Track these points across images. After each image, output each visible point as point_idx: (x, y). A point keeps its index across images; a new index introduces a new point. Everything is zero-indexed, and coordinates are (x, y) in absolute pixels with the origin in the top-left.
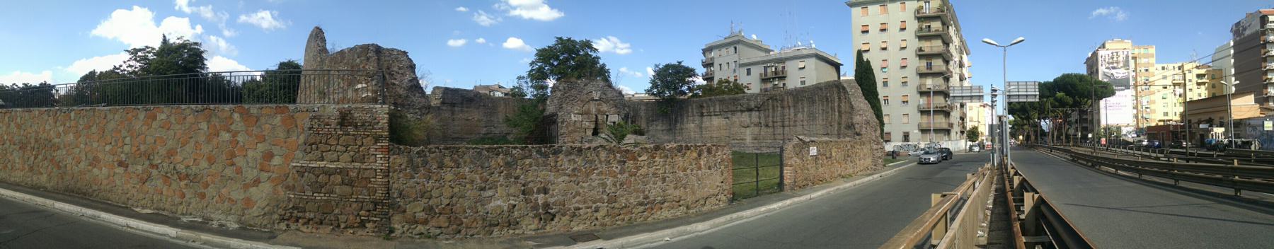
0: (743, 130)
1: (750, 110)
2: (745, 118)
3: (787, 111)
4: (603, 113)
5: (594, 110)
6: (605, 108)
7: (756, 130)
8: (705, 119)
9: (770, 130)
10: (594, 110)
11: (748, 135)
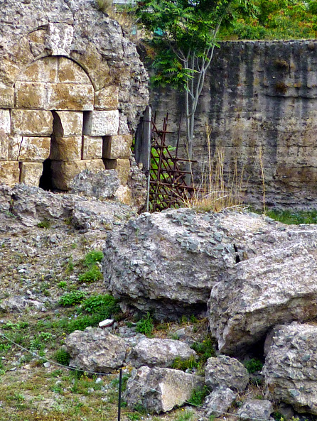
4: (75, 104)
5: (46, 97)
6: (80, 86)
8: (287, 107)
10: (46, 97)
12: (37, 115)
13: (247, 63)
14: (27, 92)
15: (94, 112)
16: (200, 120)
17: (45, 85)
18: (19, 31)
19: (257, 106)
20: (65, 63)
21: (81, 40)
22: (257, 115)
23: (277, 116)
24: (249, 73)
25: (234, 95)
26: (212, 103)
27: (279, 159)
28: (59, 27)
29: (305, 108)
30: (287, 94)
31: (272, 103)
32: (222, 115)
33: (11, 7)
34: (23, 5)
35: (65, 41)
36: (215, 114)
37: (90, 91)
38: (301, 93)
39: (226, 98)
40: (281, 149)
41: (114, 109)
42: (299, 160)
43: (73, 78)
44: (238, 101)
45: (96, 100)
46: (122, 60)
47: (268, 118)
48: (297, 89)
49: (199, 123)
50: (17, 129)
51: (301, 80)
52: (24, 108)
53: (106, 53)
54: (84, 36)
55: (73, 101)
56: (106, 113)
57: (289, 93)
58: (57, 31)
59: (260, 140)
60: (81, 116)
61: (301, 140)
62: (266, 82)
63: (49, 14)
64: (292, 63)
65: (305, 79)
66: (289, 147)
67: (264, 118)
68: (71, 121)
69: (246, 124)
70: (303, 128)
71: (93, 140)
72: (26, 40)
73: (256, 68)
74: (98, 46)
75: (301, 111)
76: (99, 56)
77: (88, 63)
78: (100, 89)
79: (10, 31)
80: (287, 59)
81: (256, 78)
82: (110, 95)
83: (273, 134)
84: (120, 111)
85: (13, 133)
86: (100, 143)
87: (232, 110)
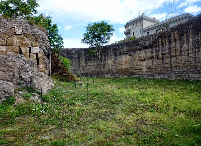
0: (141, 62)
1: (145, 48)
2: (142, 54)
3: (173, 44)
4: (26, 45)
7: (150, 62)
8: (118, 57)
9: (160, 61)
12: (14, 47)
13: (110, 49)
14: (10, 42)
15: (32, 47)
17: (16, 41)
18: (6, 28)
19: (112, 58)
20: (22, 36)
21: (25, 31)
22: (113, 59)
24: (110, 51)
25: (108, 56)
26: (104, 58)
27: (117, 68)
28: (18, 27)
29: (121, 57)
30: (117, 54)
31: (115, 56)
32: (106, 60)
33: (2, 22)
34: (7, 23)
35: (20, 30)
36: (105, 60)
37: (30, 42)
38: (120, 54)
39: (107, 57)
40: (117, 66)
41: (37, 47)
43: (24, 39)
44: (109, 57)
45: (32, 45)
46: (37, 35)
47: (114, 60)
48: (119, 53)
50: (7, 50)
52: (10, 46)
53: (33, 34)
54: (26, 30)
55: (25, 44)
56: (35, 48)
57: (118, 54)
58: (17, 28)
59: (113, 64)
60: (28, 49)
62: (113, 53)
63: (15, 25)
64: (118, 48)
65: (120, 50)
68: (25, 49)
69: (111, 61)
71: (32, 54)
72: (9, 30)
73: (111, 50)
74: (30, 32)
76: (31, 34)
77: (28, 36)
78: (33, 42)
79: (3, 28)
80: (116, 47)
81: (112, 52)
82: (36, 43)
83: (115, 63)
84: (40, 47)
85: (6, 51)
86: (35, 55)
87: (108, 59)
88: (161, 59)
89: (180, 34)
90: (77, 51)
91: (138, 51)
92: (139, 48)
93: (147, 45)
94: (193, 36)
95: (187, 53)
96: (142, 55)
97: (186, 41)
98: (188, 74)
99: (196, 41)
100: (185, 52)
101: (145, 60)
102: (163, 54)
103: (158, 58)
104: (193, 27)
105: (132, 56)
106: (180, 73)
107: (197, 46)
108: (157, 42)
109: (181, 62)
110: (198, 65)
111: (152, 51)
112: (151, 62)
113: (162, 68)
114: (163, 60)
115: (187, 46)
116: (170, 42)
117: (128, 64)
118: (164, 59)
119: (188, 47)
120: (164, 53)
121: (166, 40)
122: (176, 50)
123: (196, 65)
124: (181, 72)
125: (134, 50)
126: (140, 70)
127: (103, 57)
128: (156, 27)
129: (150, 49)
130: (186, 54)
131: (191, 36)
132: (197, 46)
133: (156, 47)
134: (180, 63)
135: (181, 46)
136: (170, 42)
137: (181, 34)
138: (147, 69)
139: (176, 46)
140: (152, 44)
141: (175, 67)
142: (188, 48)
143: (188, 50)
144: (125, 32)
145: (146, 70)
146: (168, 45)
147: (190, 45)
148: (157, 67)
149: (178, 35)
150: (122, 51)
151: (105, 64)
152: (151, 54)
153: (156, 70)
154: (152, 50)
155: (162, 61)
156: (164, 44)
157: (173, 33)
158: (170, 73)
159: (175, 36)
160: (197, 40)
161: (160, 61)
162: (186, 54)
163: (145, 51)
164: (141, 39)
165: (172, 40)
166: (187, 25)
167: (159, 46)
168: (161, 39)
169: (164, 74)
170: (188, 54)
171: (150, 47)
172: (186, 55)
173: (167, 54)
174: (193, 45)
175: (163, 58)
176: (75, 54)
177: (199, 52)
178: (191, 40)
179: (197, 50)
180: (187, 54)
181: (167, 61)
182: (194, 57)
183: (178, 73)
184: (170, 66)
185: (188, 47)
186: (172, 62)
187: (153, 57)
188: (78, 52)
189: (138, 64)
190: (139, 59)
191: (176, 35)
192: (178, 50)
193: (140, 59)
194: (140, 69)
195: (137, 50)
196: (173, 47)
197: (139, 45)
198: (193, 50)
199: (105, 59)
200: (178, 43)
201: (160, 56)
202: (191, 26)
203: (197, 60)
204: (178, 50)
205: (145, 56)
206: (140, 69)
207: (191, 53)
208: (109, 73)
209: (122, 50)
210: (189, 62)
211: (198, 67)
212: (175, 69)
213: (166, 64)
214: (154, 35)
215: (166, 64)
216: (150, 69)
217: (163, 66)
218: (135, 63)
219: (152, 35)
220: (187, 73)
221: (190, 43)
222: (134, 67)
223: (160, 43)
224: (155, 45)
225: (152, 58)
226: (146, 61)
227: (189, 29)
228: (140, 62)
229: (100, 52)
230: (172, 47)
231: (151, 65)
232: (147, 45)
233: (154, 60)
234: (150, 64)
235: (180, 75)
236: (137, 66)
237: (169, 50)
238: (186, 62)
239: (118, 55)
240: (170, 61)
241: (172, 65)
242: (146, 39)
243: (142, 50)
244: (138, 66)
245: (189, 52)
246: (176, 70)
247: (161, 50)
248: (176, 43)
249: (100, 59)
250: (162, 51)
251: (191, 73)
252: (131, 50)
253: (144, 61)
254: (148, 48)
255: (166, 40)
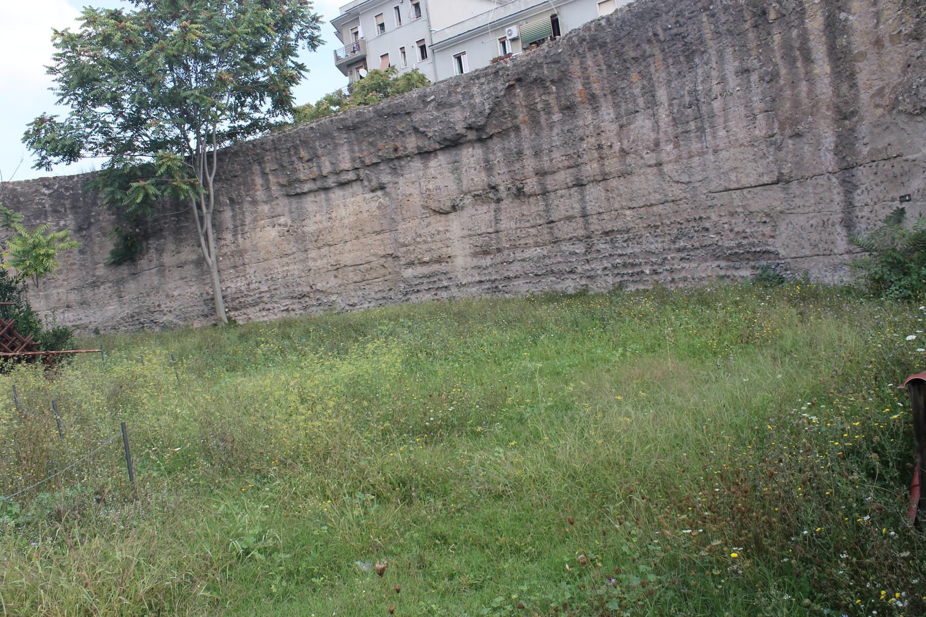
0: (438, 223)
1: (453, 143)
3: (586, 117)
7: (483, 215)
8: (309, 203)
9: (534, 207)
11: (457, 237)
13: (260, 164)
16: (225, 239)
19: (279, 210)
22: (282, 220)
23: (301, 217)
24: (264, 174)
25: (254, 202)
26: (234, 217)
29: (327, 200)
32: (246, 229)
38: (319, 184)
39: (247, 206)
42: (332, 262)
47: (293, 221)
49: (223, 242)
51: (315, 169)
61: (329, 238)
65: (319, 167)
66: (319, 248)
67: (289, 222)
69: (272, 233)
70: (329, 224)
75: (324, 204)
88: (536, 195)
89: (609, 66)
90: (67, 189)
91: (417, 164)
92: (418, 148)
93: (460, 128)
94: (669, 74)
95: (653, 162)
96: (439, 182)
97: (641, 102)
98: (668, 267)
99: (687, 99)
100: (642, 158)
101: (454, 208)
102: (541, 174)
103: (520, 194)
104: (666, 30)
105: (386, 194)
106: (633, 265)
107: (692, 125)
108: (506, 107)
109: (630, 208)
110: (709, 218)
111: (487, 161)
112: (487, 217)
113: (545, 244)
114: (544, 200)
115: (648, 124)
116: (569, 109)
117: (369, 240)
118: (552, 195)
119: (654, 131)
120: (546, 165)
121: (552, 100)
122: (600, 147)
123: (701, 218)
124: (635, 255)
125: (392, 160)
126: (435, 267)
127: (228, 214)
128: (499, 26)
129: (477, 145)
130: (650, 166)
131: (663, 75)
132: (692, 125)
133: (503, 134)
134: (628, 212)
135: (621, 127)
136: (569, 109)
137: (614, 69)
138: (475, 255)
139: (599, 127)
140: (481, 121)
141: (606, 233)
142: (653, 136)
143: (657, 144)
144: (337, 58)
145: (469, 259)
146: (563, 122)
147: (663, 113)
148: (523, 242)
149: (605, 73)
150: (327, 168)
151: (241, 253)
152: (483, 174)
153: (519, 255)
154: (485, 153)
155: (541, 208)
156: (543, 118)
157: (577, 61)
158: (587, 267)
159: (588, 78)
160: (690, 93)
161: (534, 209)
162: (650, 166)
163: (453, 159)
164: (425, 96)
165: (580, 99)
166: (640, 22)
167: (517, 129)
168: (527, 96)
169: (561, 273)
170: (659, 164)
171: (472, 135)
172: (649, 170)
173: (562, 172)
174: (674, 119)
175: (545, 193)
176: (55, 211)
177: (707, 153)
178: (662, 94)
179: (695, 146)
180: (656, 165)
181: (565, 204)
182: (685, 178)
183: (625, 265)
184: (581, 232)
185: (656, 128)
186: (589, 208)
187: (494, 188)
188: (75, 198)
189: (422, 232)
190: (425, 207)
191: (593, 73)
192: (611, 146)
193: (434, 205)
194: (439, 260)
195: (407, 156)
196: (587, 133)
197: (416, 130)
198: (677, 146)
199: (238, 222)
200: (607, 112)
201: (532, 185)
202: (660, 32)
203: (702, 193)
204: (611, 146)
205: (453, 186)
206: (439, 260)
207: (670, 161)
208: (272, 297)
209: (327, 164)
210: (670, 207)
211: (707, 230)
212: (607, 246)
213: (560, 220)
214: (486, 75)
215: (560, 220)
216: (486, 253)
217: (551, 234)
218: (408, 229)
219: (478, 77)
220: (665, 259)
221: (661, 110)
222: (404, 249)
223: (522, 115)
224: (496, 127)
225: (489, 194)
226: (466, 213)
227: (649, 41)
228: (434, 219)
229: (206, 185)
230: (580, 132)
231: (491, 230)
232: (460, 128)
233: (505, 204)
234: (484, 229)
235: (632, 275)
236: (419, 243)
237: (571, 152)
238: (652, 205)
239: (310, 191)
240: (577, 206)
241: (592, 228)
242: (450, 94)
243: (436, 156)
244: (425, 242)
245: (664, 157)
246: (611, 251)
247: (528, 152)
248: (596, 110)
249: (213, 225)
250: (537, 154)
251: (681, 259)
252: (375, 161)
253: (452, 216)
254: (461, 144)
255: (552, 100)
